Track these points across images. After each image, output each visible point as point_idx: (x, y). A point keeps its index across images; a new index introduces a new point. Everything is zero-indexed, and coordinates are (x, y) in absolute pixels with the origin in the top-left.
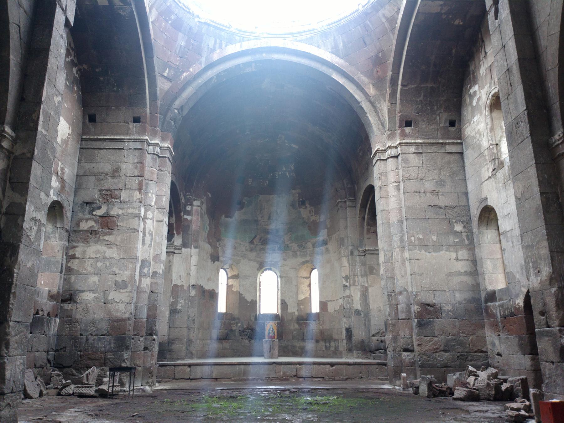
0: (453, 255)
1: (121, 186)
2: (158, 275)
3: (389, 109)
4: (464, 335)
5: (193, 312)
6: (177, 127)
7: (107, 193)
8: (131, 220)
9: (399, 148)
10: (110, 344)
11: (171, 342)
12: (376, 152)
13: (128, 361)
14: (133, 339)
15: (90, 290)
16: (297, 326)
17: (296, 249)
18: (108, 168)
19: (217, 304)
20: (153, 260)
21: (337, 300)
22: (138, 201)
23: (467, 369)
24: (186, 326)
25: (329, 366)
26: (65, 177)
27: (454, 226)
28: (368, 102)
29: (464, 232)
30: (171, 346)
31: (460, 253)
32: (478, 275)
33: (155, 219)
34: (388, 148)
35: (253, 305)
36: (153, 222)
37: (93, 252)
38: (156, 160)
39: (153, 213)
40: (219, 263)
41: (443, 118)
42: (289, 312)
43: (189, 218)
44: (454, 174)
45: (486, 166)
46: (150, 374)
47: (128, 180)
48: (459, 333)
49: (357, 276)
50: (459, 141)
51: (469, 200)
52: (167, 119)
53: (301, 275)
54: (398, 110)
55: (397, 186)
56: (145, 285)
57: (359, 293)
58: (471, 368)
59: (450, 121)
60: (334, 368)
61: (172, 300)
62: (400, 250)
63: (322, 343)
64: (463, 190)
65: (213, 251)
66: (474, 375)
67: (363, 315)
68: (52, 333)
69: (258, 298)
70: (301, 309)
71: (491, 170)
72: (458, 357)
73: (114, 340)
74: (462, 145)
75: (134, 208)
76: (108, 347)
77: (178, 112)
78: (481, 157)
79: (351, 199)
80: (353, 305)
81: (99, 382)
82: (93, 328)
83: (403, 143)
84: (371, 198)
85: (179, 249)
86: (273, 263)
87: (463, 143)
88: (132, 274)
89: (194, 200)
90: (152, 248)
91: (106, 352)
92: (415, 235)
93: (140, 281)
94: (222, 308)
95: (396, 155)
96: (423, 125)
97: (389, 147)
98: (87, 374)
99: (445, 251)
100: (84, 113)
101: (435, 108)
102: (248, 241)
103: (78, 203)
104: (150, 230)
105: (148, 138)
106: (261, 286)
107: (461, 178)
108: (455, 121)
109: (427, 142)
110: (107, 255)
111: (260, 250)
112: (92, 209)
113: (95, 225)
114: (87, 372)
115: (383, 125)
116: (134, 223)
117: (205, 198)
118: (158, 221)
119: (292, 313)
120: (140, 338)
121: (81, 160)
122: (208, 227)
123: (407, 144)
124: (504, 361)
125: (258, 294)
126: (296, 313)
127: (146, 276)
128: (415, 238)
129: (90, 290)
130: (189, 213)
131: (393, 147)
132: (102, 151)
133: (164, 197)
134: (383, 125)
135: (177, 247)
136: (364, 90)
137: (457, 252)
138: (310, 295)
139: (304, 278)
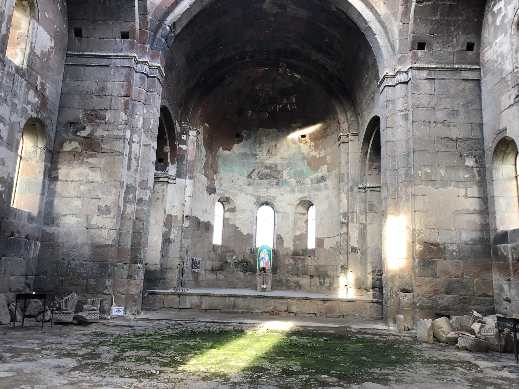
0: (462, 192)
1: (106, 105)
2: (144, 202)
3: (400, 29)
4: (469, 277)
5: (186, 243)
6: (169, 46)
7: (92, 113)
8: (115, 143)
9: (410, 73)
10: (92, 270)
11: (164, 270)
12: (383, 77)
13: (110, 288)
14: (116, 266)
15: (72, 214)
16: (292, 261)
17: (294, 184)
18: (94, 87)
19: (212, 236)
20: (139, 186)
21: (333, 237)
22: (123, 122)
23: (472, 314)
24: (179, 256)
25: (320, 303)
26: (47, 93)
27: (465, 160)
28: (378, 23)
29: (476, 167)
30: (164, 275)
31: (469, 189)
32: (488, 214)
33: (142, 143)
34: (397, 73)
35: (249, 238)
36: (140, 146)
37: (77, 175)
38: (144, 81)
39: (140, 137)
40: (216, 195)
41: (463, 39)
42: (285, 247)
43: (184, 147)
44: (469, 103)
45: (508, 93)
46: (134, 302)
47: (113, 99)
48: (463, 274)
49: (356, 213)
50: (477, 67)
51: (484, 133)
52: (158, 36)
53: (298, 211)
54: (410, 30)
55: (405, 115)
56: (130, 212)
57: (357, 231)
58: (475, 313)
59: (468, 43)
60: (326, 304)
61: (165, 230)
62: (404, 185)
63: (316, 279)
64: (478, 121)
65: (209, 183)
66: (480, 322)
67: (359, 253)
68: (32, 256)
69: (254, 232)
71: (513, 97)
72: (460, 300)
73: (96, 266)
74: (480, 71)
75: (119, 130)
76: (90, 273)
77: (170, 29)
78: (502, 83)
79: (354, 133)
80: (350, 243)
81: (79, 308)
82: (75, 253)
83: (414, 68)
84: (375, 132)
85: (173, 179)
86: (270, 197)
87: (482, 69)
88: (116, 200)
89: (190, 129)
90: (138, 173)
91: (88, 278)
92: (422, 168)
93: (125, 207)
94: (217, 239)
95: (407, 81)
96: (437, 47)
97: (398, 72)
98: (66, 300)
99: (454, 187)
100: (70, 26)
101: (453, 29)
102: (245, 175)
103: (62, 123)
104: (136, 154)
105: (135, 55)
107: (476, 108)
108: (474, 43)
109: (441, 67)
110: (90, 178)
111: (258, 184)
112: (76, 130)
113: (79, 146)
114: (66, 298)
115: (393, 48)
116: (119, 146)
117: (202, 128)
118: (145, 145)
119: (288, 248)
120: (124, 265)
121: (66, 77)
122: (205, 159)
123: (419, 69)
124: (513, 308)
125: (254, 228)
126: (292, 249)
127: (130, 202)
128: (421, 172)
129: (72, 214)
130: (184, 142)
131: (403, 72)
132: (88, 68)
133: (152, 120)
134: (393, 48)
135: (171, 177)
136: (374, 9)
137: (466, 189)
138: (307, 231)
139: (301, 214)
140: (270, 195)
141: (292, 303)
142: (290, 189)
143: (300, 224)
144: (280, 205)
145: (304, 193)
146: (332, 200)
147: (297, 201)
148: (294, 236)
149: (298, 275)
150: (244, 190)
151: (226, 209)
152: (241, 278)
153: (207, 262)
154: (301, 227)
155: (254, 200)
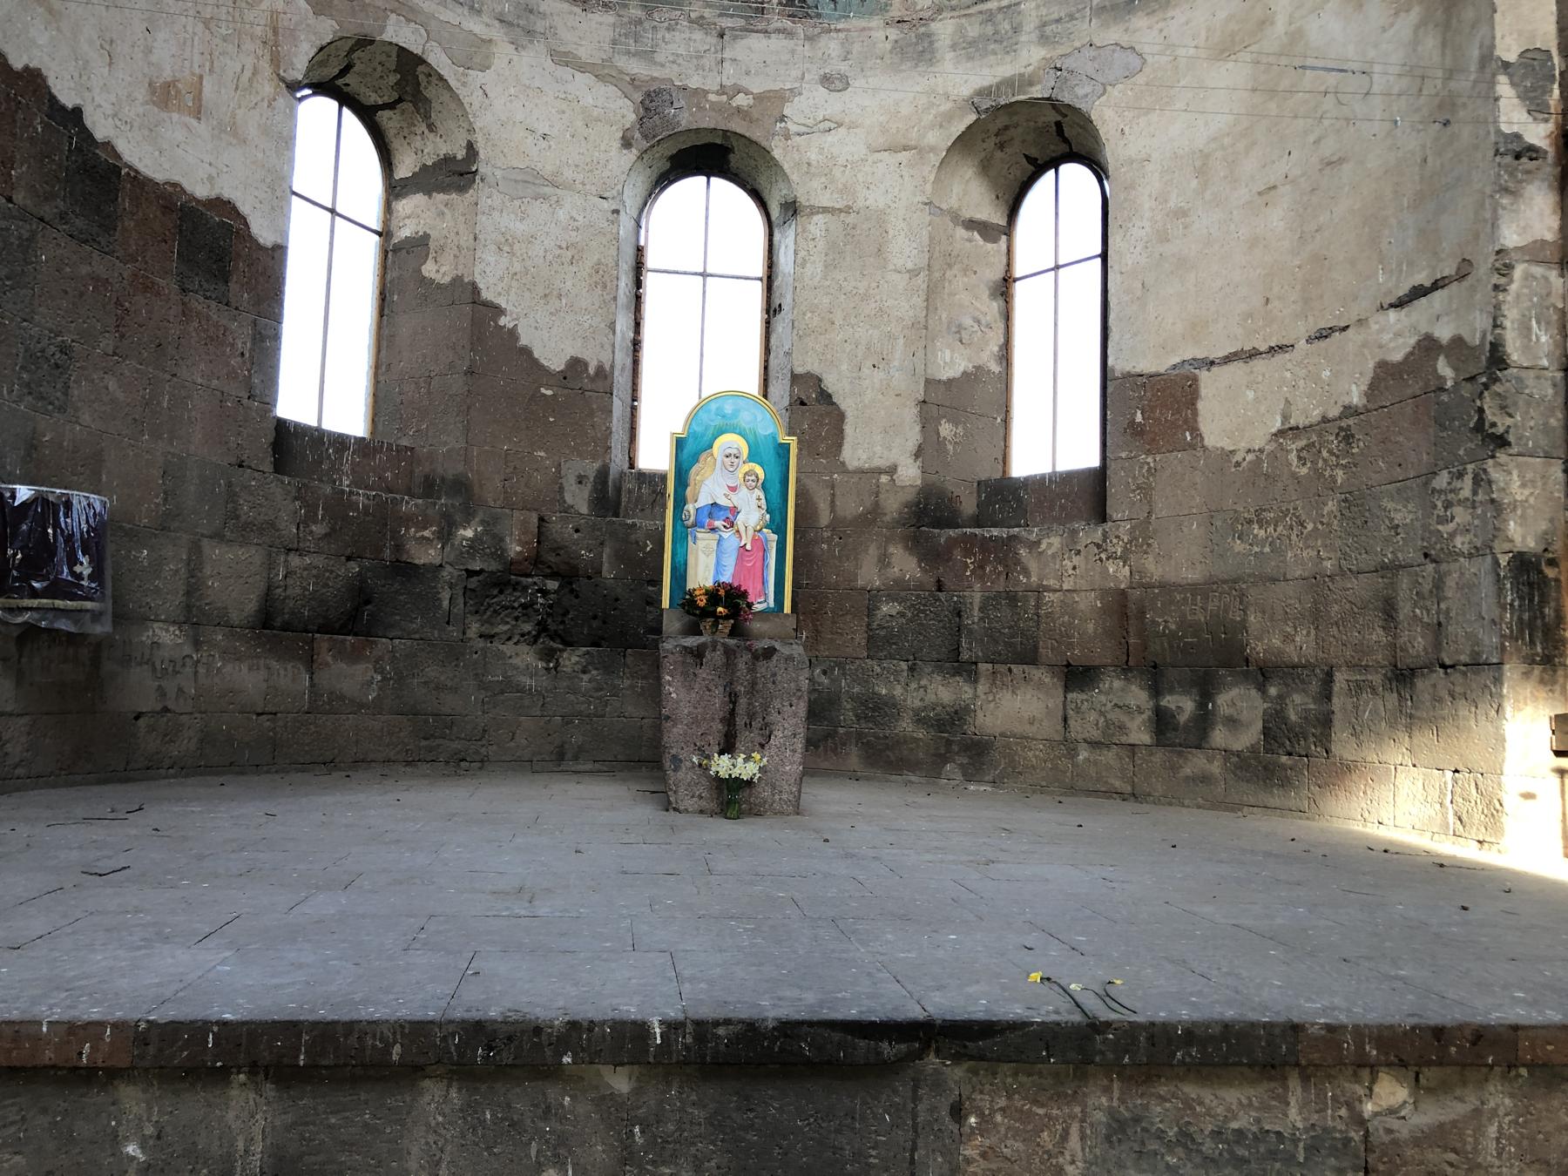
21: (1322, 335)
53: (953, 202)
70: (940, 443)
86: (741, 100)
106: (650, 280)
119: (879, 471)
126: (910, 473)
138: (1006, 355)
139: (971, 224)
140: (745, 82)
141: (1439, 1136)
142: (893, 33)
143: (964, 297)
144: (813, 156)
145: (1011, 49)
146: (1296, 36)
147: (949, 117)
148: (928, 382)
149: (958, 666)
150: (540, 26)
151: (405, 168)
152: (520, 689)
153: (217, 555)
154: (968, 322)
155: (627, 113)
